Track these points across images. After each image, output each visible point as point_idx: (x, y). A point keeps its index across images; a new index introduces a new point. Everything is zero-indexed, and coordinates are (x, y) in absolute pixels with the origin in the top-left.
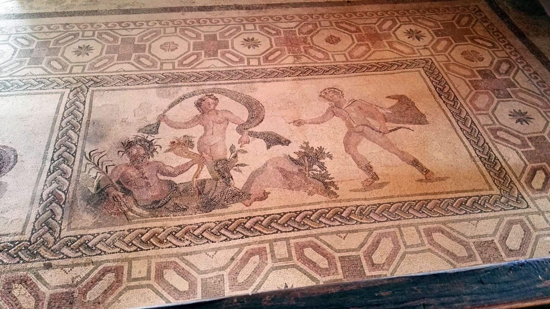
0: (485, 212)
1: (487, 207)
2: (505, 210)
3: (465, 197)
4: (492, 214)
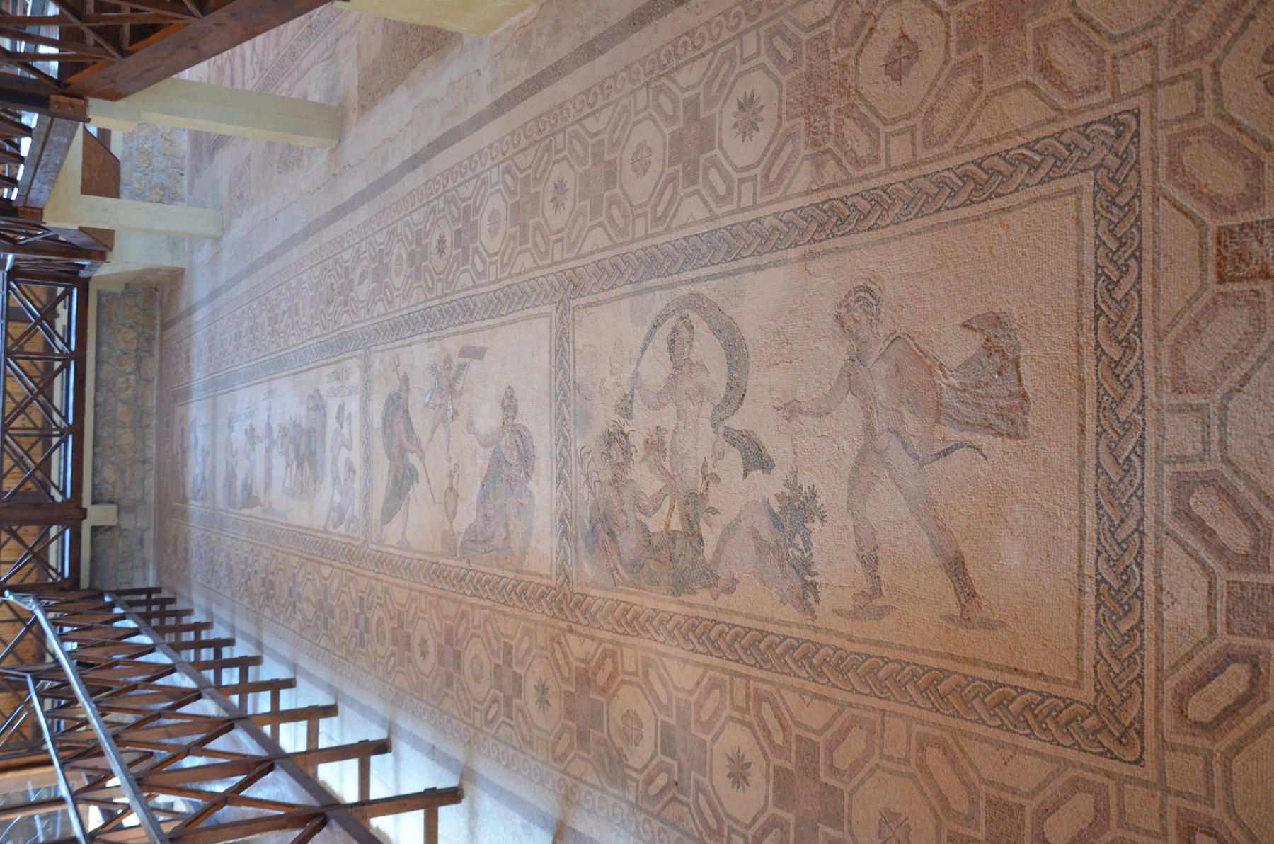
0: (1037, 738)
1: (1047, 729)
2: (1080, 749)
3: (1015, 688)
4: (1049, 749)
